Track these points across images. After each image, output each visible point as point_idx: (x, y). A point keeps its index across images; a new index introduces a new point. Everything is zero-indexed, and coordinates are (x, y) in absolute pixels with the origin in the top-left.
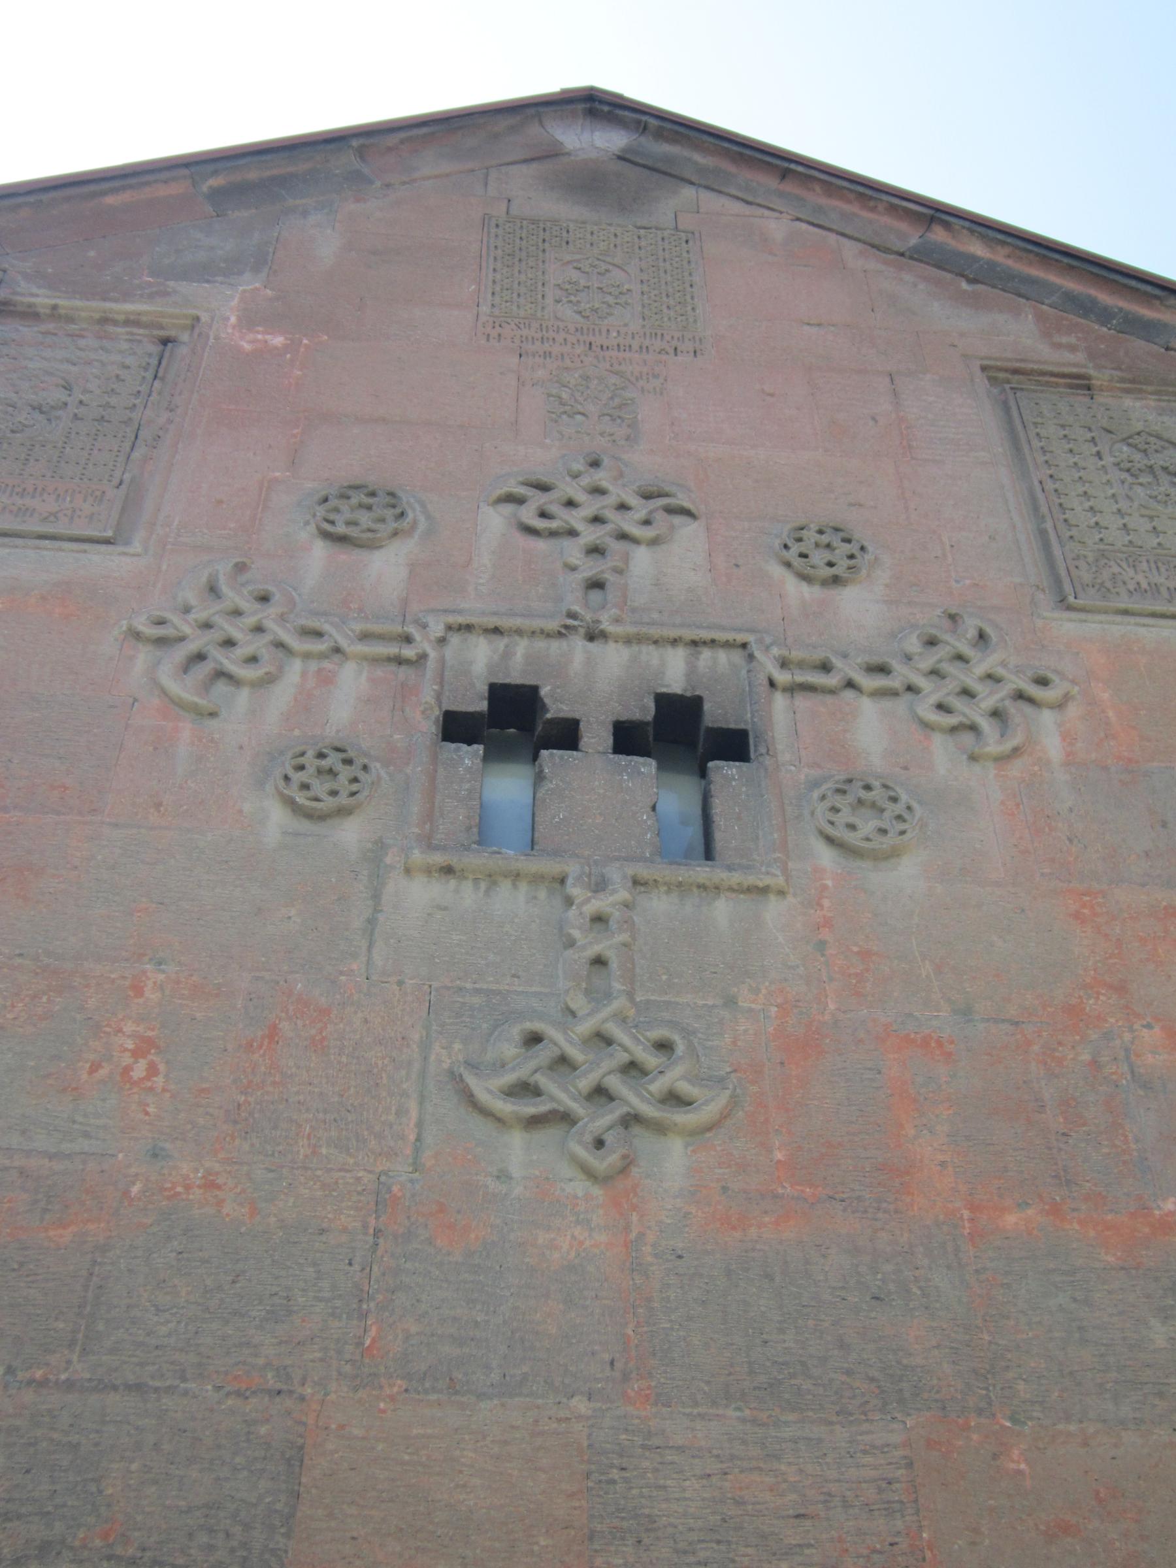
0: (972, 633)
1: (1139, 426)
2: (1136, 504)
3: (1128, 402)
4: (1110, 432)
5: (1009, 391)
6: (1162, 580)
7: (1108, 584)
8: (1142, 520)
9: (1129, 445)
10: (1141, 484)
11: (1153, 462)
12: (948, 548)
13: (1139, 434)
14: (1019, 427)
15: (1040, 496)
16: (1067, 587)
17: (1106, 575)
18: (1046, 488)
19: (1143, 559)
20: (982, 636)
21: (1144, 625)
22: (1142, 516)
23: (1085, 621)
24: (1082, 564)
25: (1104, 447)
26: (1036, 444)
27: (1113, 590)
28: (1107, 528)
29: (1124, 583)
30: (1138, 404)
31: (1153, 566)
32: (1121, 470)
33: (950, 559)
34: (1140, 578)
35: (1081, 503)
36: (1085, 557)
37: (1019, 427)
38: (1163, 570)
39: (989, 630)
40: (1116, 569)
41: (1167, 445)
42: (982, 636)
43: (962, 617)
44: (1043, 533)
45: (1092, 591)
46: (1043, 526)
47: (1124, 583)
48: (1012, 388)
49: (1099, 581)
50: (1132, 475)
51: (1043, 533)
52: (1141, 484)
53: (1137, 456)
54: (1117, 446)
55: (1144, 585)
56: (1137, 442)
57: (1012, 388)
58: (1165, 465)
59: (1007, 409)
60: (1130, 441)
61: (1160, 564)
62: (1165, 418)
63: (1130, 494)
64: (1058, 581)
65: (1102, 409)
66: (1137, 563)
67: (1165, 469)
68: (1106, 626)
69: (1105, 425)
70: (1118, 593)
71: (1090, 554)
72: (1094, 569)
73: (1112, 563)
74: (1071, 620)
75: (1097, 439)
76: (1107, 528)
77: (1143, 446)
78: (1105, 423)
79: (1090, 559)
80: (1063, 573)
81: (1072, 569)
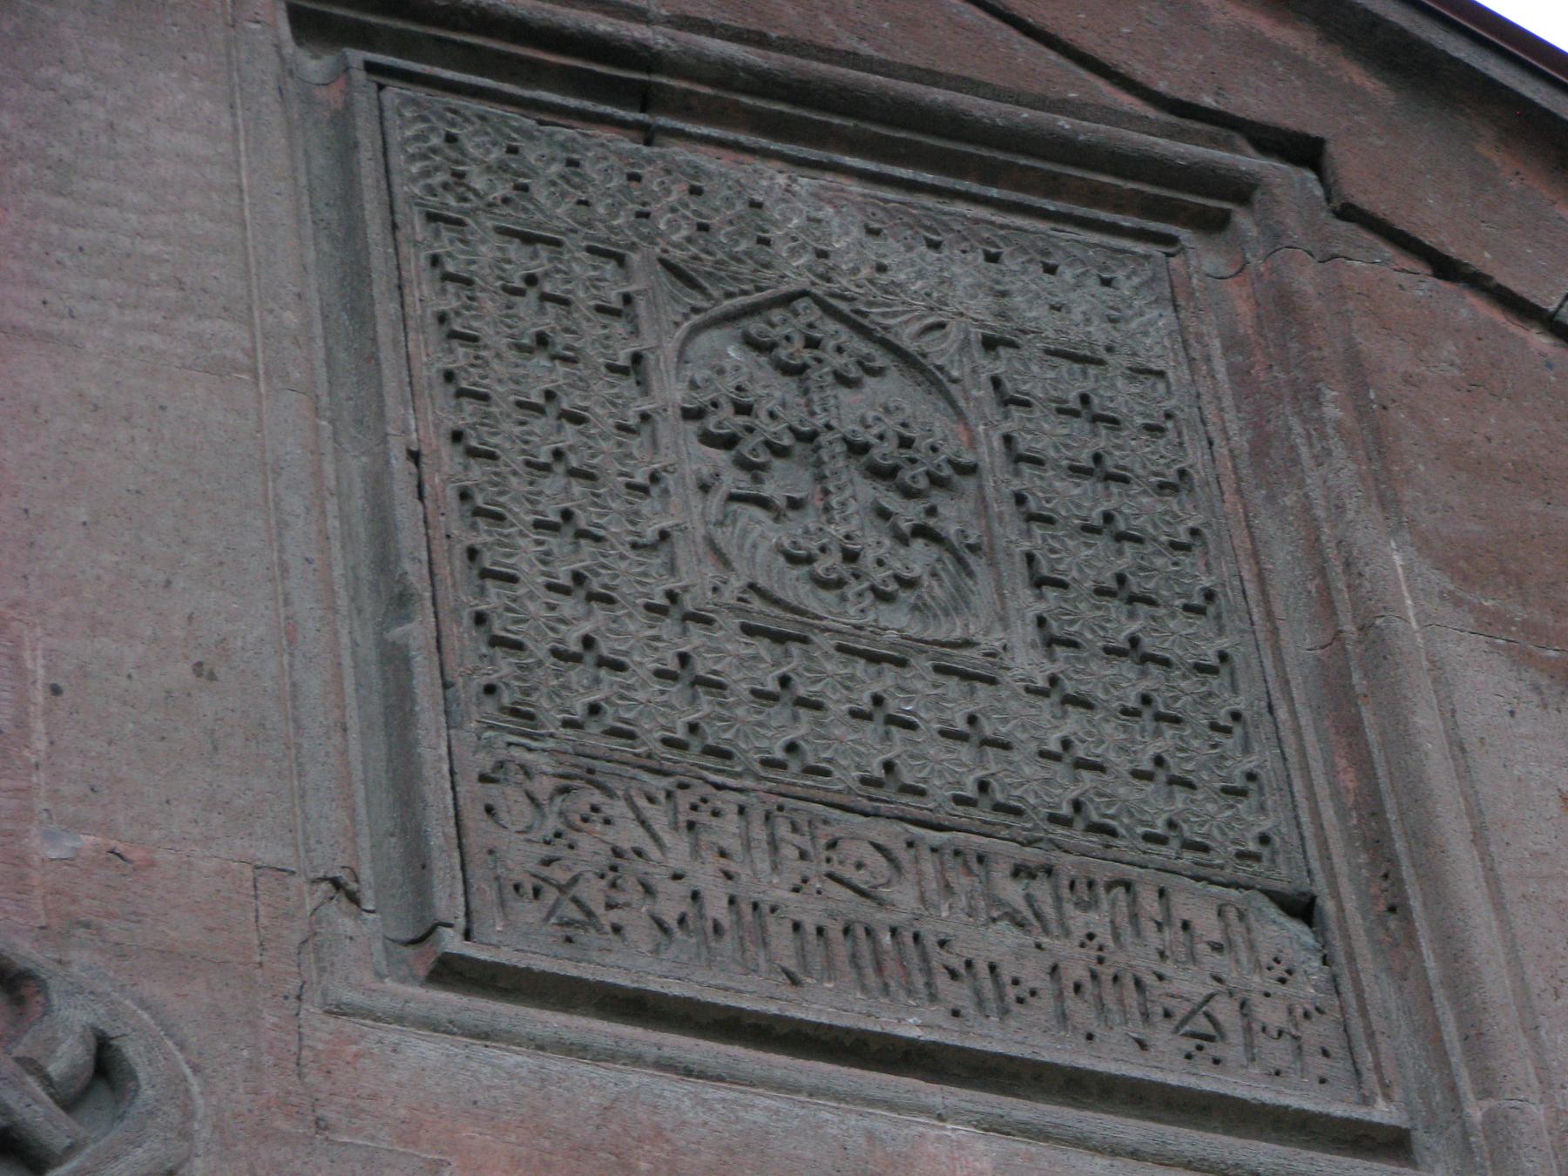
0: (68, 1057)
1: (795, 271)
2: (737, 583)
3: (772, 179)
4: (691, 283)
5: (360, 76)
6: (782, 894)
7: (593, 892)
8: (741, 647)
9: (751, 343)
10: (763, 503)
11: (820, 420)
12: (39, 696)
13: (787, 300)
14: (375, 229)
15: (406, 510)
16: (447, 901)
17: (591, 848)
18: (434, 481)
19: (728, 802)
20: (106, 1067)
21: (688, 1072)
22: (749, 630)
23: (485, 1035)
24: (510, 798)
25: (660, 332)
26: (426, 296)
27: (607, 918)
28: (618, 667)
29: (648, 890)
30: (805, 183)
31: (759, 833)
32: (708, 439)
33: (41, 745)
34: (705, 876)
35: (546, 558)
36: (527, 772)
37: (375, 229)
38: (789, 852)
39: (132, 1051)
40: (629, 835)
41: (881, 359)
42: (106, 1067)
43: (42, 988)
44: (395, 660)
45: (529, 912)
46: (396, 633)
47: (648, 890)
48: (371, 67)
49: (558, 874)
50: (743, 464)
51: (395, 660)
52: (763, 503)
53: (772, 391)
54: (705, 341)
55: (716, 908)
56: (777, 333)
57: (371, 67)
58: (862, 437)
59: (346, 150)
60: (754, 326)
61: (783, 830)
62: (891, 250)
63: (719, 535)
64: (418, 863)
65: (678, 192)
66: (703, 816)
67: (857, 449)
68: (556, 1065)
69: (677, 256)
70: (617, 929)
71: (542, 762)
72: (552, 823)
73: (617, 809)
74: (432, 1025)
75: (641, 305)
76: (618, 667)
77: (794, 352)
78: (676, 236)
79: (544, 786)
80: (439, 833)
81: (474, 815)
